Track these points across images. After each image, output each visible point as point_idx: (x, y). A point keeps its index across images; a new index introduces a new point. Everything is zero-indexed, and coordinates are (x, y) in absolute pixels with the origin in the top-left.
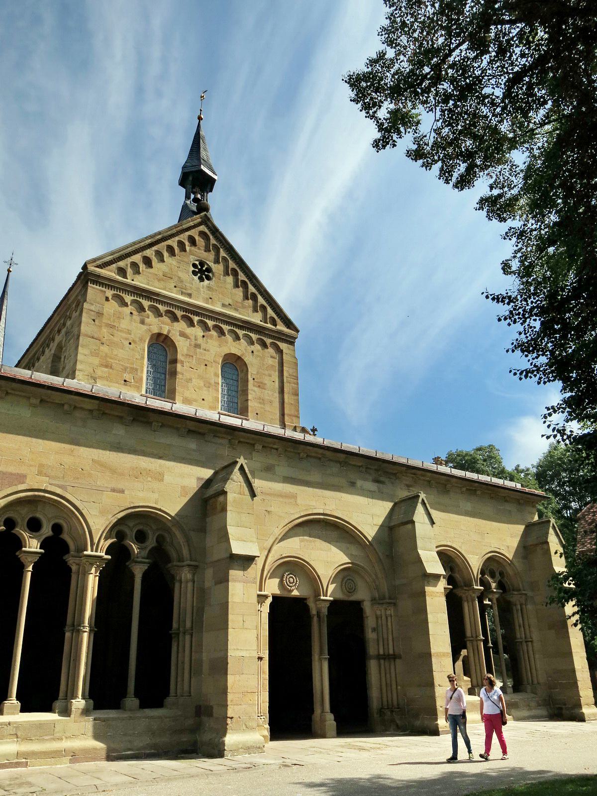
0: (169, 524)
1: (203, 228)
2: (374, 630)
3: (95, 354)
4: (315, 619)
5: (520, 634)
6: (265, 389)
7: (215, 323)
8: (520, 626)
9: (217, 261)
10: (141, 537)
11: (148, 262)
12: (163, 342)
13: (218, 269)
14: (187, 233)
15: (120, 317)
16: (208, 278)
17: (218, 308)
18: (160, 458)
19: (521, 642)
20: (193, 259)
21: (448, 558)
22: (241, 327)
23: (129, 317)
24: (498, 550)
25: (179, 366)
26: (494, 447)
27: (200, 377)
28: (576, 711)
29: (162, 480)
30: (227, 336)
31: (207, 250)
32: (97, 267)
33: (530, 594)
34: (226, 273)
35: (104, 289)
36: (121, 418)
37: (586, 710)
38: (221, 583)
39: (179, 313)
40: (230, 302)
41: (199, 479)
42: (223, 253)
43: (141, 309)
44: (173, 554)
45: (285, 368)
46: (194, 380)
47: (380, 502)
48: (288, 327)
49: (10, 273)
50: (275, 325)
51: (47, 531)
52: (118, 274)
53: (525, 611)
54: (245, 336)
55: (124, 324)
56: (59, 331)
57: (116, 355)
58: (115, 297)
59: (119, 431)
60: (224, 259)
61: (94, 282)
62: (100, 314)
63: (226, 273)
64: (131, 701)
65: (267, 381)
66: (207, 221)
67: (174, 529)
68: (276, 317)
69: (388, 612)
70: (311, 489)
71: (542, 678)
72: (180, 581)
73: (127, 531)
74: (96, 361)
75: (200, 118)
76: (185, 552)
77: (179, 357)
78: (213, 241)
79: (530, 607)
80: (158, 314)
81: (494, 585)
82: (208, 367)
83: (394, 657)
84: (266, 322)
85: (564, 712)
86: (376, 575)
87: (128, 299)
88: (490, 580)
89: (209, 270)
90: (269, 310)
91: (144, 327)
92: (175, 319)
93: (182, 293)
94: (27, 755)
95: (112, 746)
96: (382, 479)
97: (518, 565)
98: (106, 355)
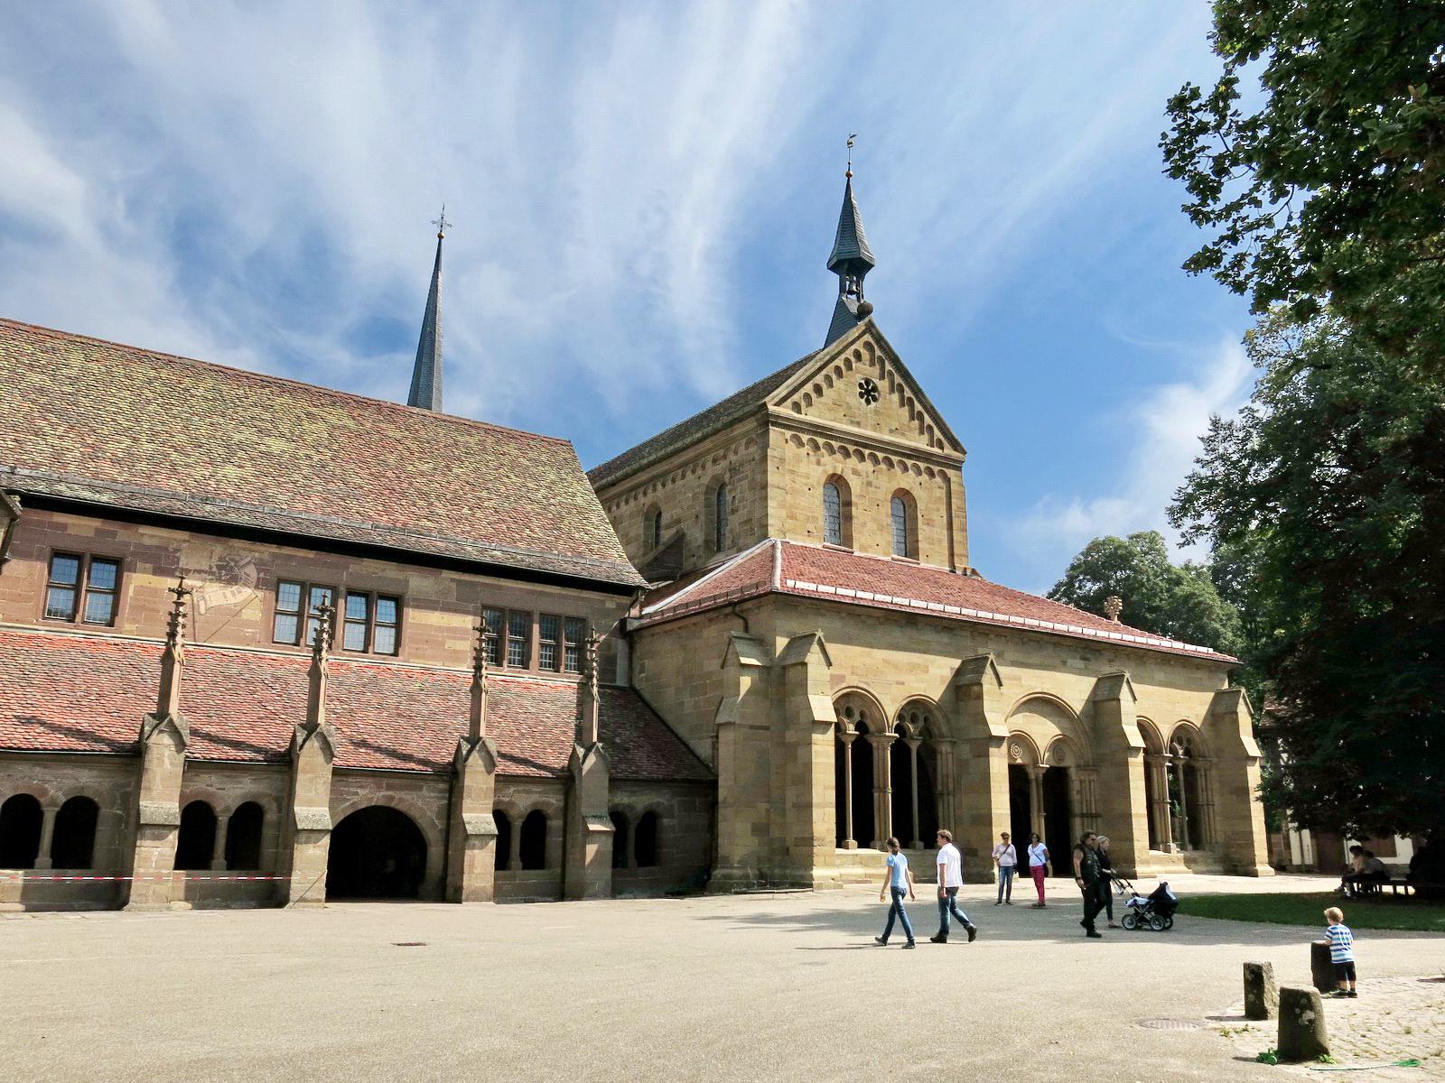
0: (933, 708)
1: (867, 337)
2: (1078, 792)
3: (782, 505)
4: (1034, 783)
5: (1202, 798)
6: (933, 526)
7: (885, 455)
8: (1202, 791)
9: (882, 377)
10: (914, 720)
11: (818, 390)
12: (836, 481)
13: (883, 385)
14: (853, 347)
15: (798, 460)
16: (875, 399)
17: (887, 437)
18: (925, 653)
19: (1203, 805)
20: (859, 379)
21: (1145, 728)
22: (909, 457)
23: (805, 460)
24: (1187, 718)
25: (854, 509)
26: (1157, 534)
27: (874, 520)
28: (1251, 868)
29: (927, 672)
30: (896, 468)
31: (872, 364)
32: (775, 405)
33: (1215, 760)
34: (892, 391)
35: (783, 430)
36: (896, 621)
37: (1259, 868)
38: (979, 756)
39: (851, 448)
40: (897, 426)
41: (952, 669)
42: (888, 367)
43: (817, 447)
44: (935, 731)
45: (953, 500)
46: (868, 524)
47: (1086, 678)
48: (955, 450)
49: (443, 240)
50: (942, 448)
51: (857, 718)
52: (793, 409)
53: (1208, 776)
54: (914, 465)
55: (803, 468)
56: (715, 461)
57: (799, 504)
58: (794, 437)
59: (897, 634)
60: (890, 373)
61: (774, 424)
62: (782, 460)
63: (892, 391)
64: (920, 844)
65: (935, 516)
66: (870, 328)
67: (935, 711)
68: (943, 439)
69: (1091, 778)
70: (1031, 671)
71: (1220, 838)
72: (942, 754)
73: (906, 715)
74: (783, 513)
75: (849, 175)
76: (945, 730)
77: (854, 499)
78: (878, 353)
79: (1214, 772)
80: (832, 451)
81: (1181, 752)
82: (880, 508)
83: (1096, 816)
84: (932, 446)
85: (1239, 868)
86: (1082, 745)
87: (805, 438)
88: (1178, 747)
89: (875, 389)
90: (936, 431)
91: (820, 469)
92: (847, 454)
93: (852, 423)
94: (871, 876)
95: (918, 873)
96: (1088, 656)
97: (1207, 734)
98: (791, 506)
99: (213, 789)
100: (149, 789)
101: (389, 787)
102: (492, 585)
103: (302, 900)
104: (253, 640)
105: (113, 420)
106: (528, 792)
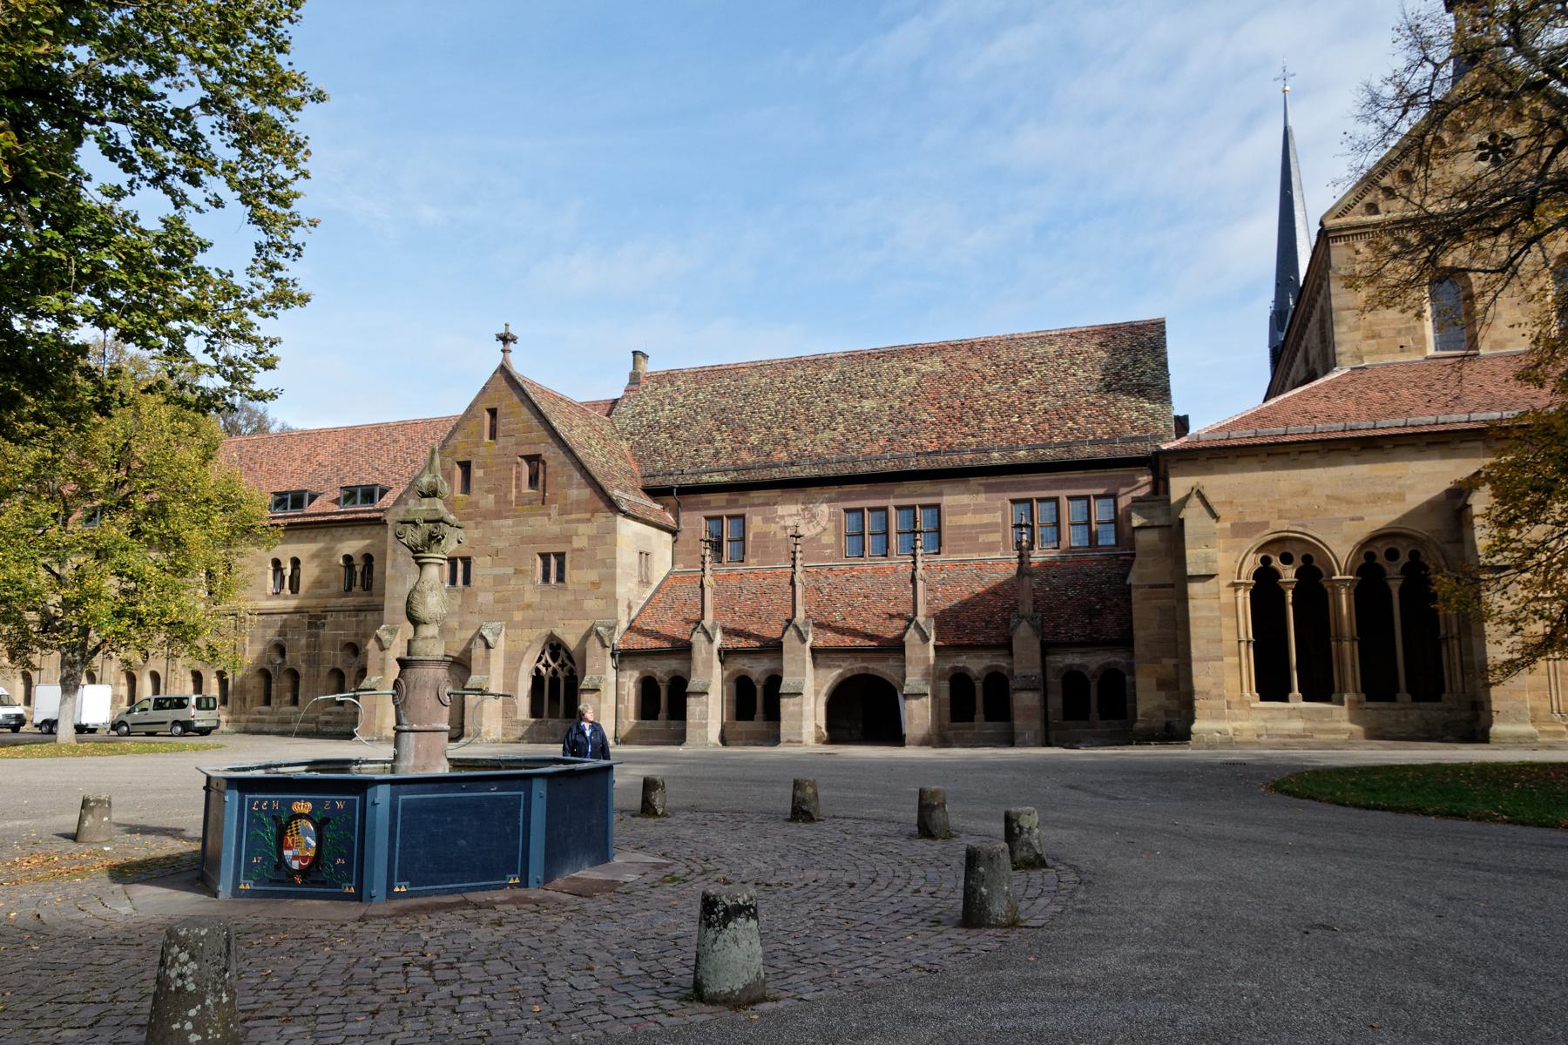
99: (745, 668)
100: (695, 669)
101: (864, 660)
102: (1013, 482)
103: (789, 741)
104: (830, 558)
105: (761, 418)
106: (980, 657)
